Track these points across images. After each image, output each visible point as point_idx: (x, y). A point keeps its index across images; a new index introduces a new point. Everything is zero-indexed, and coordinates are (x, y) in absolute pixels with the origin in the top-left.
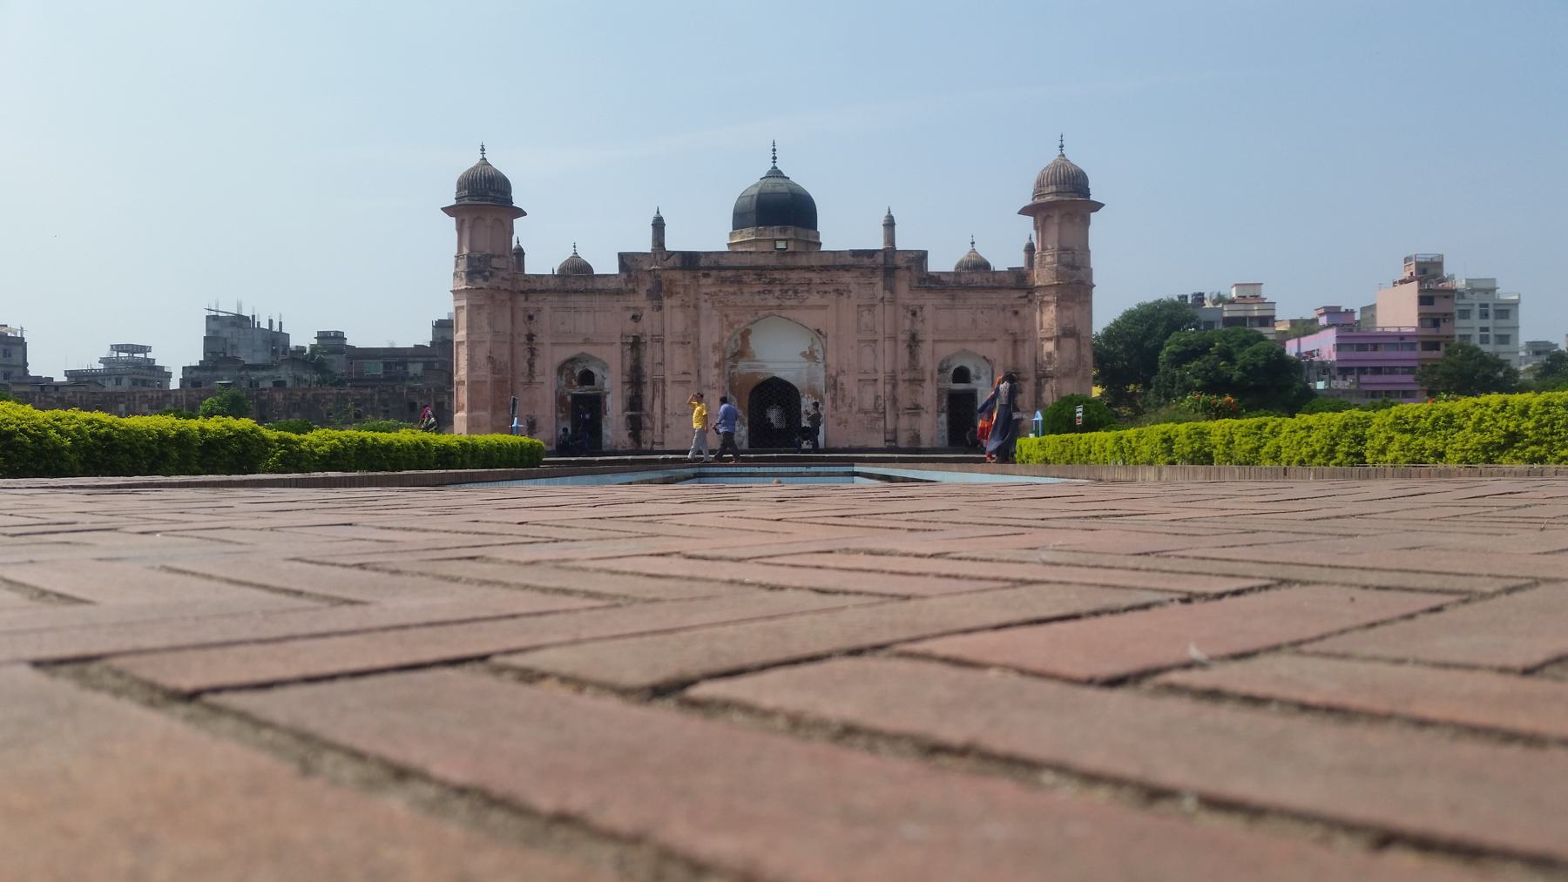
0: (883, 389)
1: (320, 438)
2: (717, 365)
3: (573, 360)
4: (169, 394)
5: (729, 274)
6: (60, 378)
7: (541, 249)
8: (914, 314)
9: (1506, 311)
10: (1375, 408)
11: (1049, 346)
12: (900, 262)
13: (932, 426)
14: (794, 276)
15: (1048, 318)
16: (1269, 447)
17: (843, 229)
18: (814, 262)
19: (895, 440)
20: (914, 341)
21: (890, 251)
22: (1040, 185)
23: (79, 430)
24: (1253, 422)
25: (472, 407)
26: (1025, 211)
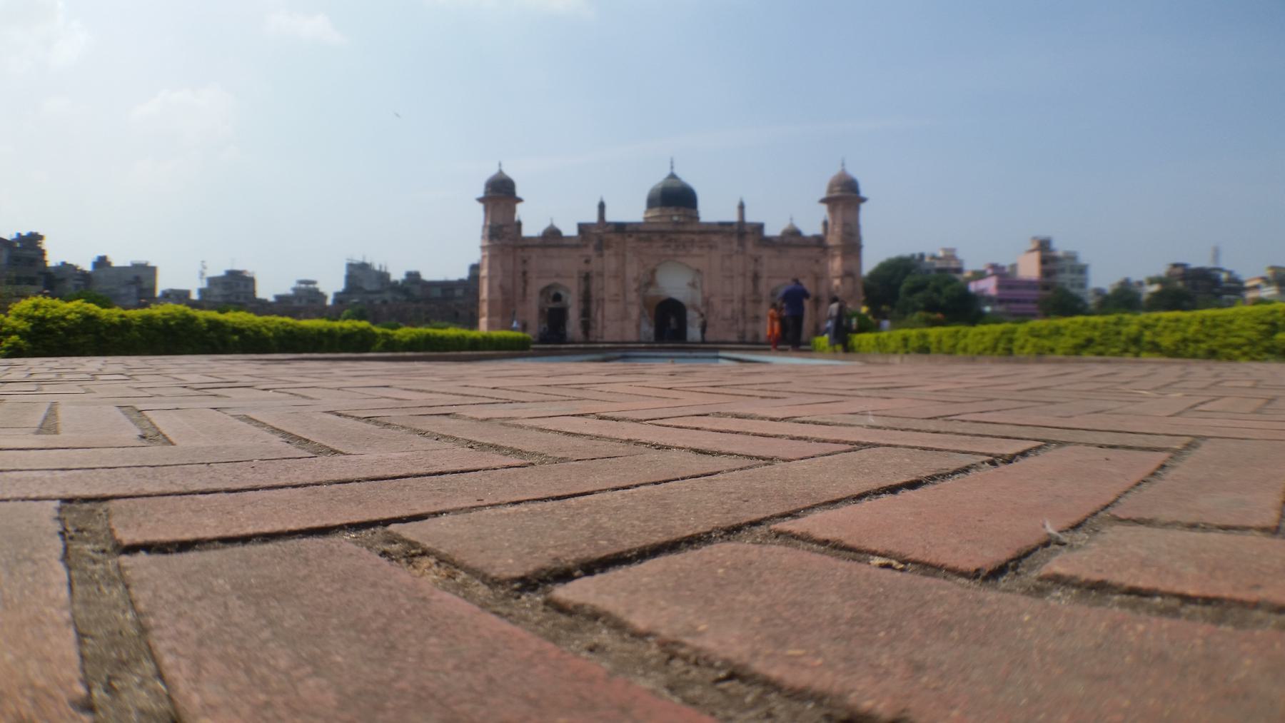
0: (737, 306)
1: (404, 332)
2: (636, 290)
3: (549, 287)
4: (326, 308)
5: (643, 235)
6: (271, 299)
7: (532, 221)
8: (756, 260)
9: (1082, 270)
10: (1019, 322)
11: (837, 282)
12: (748, 229)
13: (766, 328)
14: (683, 237)
15: (836, 265)
16: (961, 344)
17: (713, 210)
18: (695, 228)
19: (744, 336)
20: (756, 277)
21: (742, 223)
22: (831, 188)
23: (277, 328)
24: (951, 329)
25: (491, 315)
26: (824, 201)
